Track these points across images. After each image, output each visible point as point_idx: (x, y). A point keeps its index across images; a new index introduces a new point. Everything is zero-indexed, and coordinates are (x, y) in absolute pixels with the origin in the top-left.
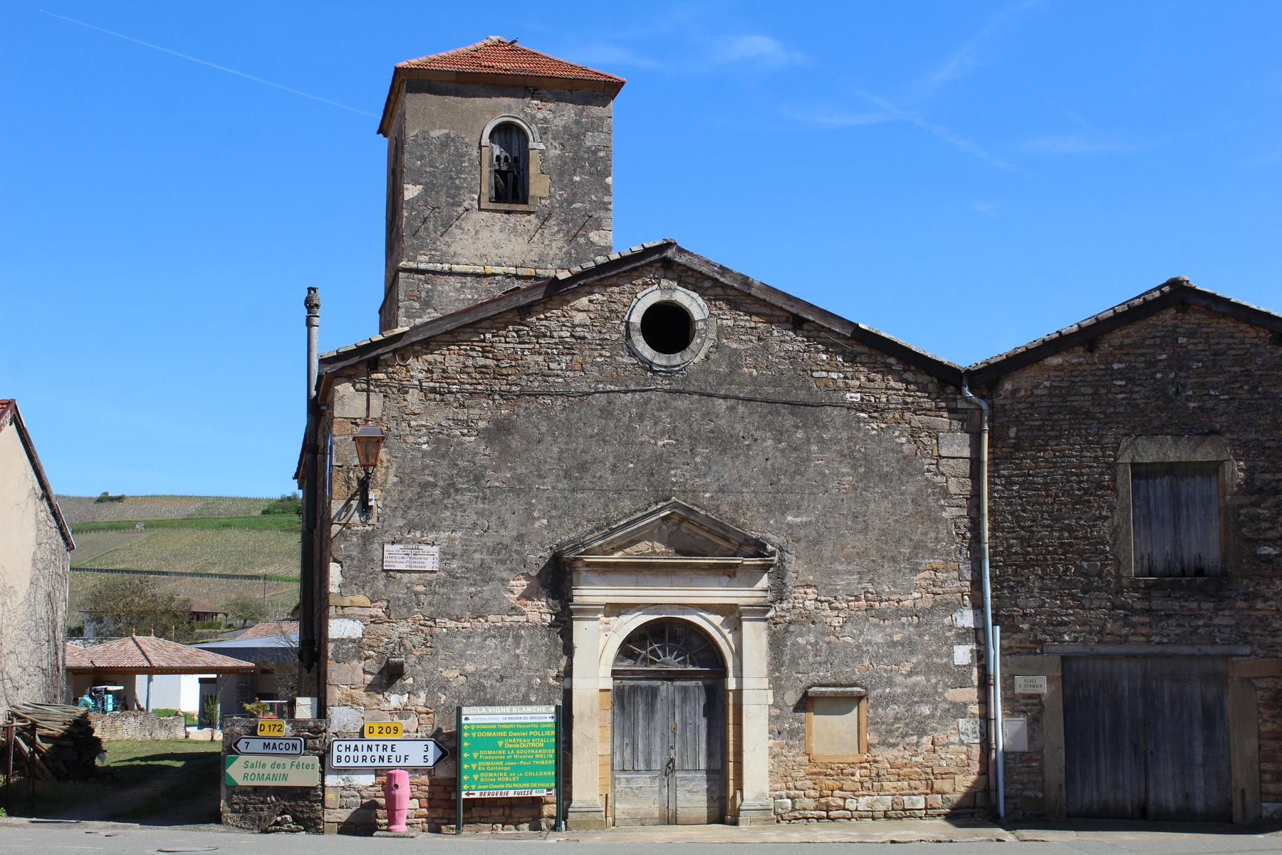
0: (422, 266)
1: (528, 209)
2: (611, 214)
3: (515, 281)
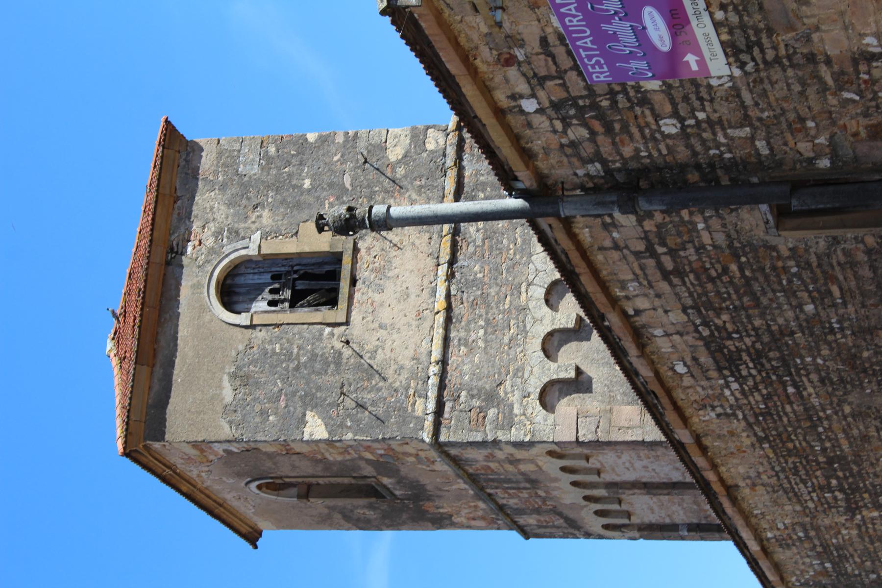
0: (431, 406)
1: (350, 252)
2: (363, 132)
3: (459, 264)
